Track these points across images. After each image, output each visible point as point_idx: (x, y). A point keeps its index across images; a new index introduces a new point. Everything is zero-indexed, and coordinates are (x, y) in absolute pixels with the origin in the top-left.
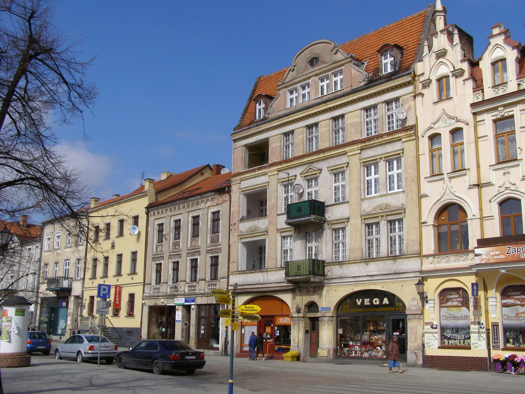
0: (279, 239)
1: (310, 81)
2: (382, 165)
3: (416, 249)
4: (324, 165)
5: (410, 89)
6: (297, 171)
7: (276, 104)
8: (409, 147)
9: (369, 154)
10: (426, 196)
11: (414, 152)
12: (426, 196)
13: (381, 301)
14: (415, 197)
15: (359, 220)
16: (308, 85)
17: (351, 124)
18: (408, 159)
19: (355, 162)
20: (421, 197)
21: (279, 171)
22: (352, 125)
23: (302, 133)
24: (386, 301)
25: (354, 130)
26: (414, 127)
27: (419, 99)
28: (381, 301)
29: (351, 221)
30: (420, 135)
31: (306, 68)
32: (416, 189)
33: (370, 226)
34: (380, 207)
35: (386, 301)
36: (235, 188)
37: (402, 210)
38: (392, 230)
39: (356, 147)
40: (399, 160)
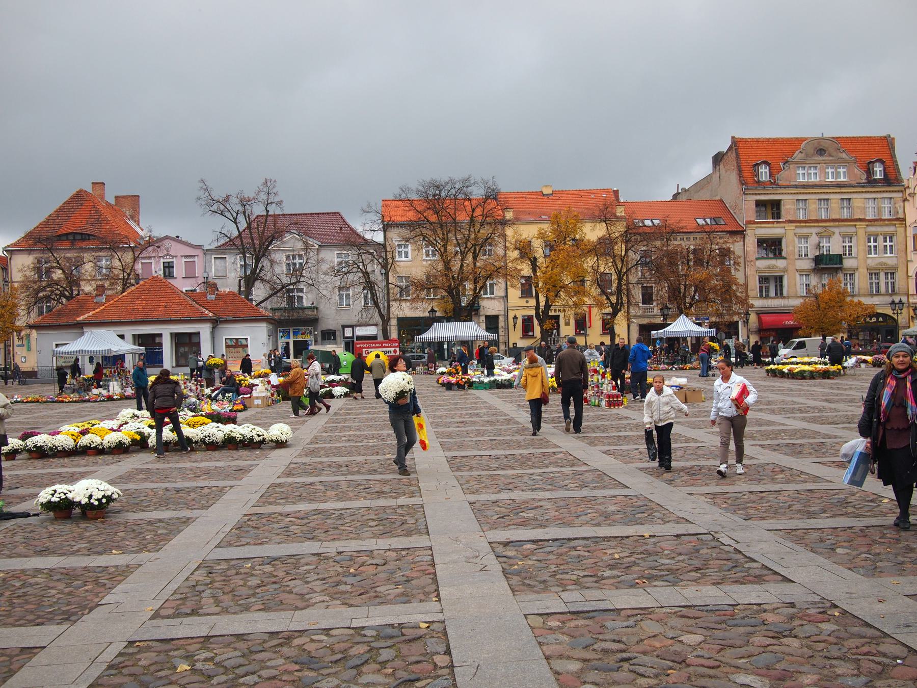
0: (798, 276)
1: (819, 166)
2: (881, 239)
3: (905, 290)
4: (837, 231)
5: (900, 195)
6: (814, 231)
7: (783, 174)
8: (900, 230)
9: (872, 229)
10: (911, 261)
11: (904, 234)
12: (911, 261)
13: (878, 319)
14: (905, 262)
15: (865, 271)
16: (816, 167)
17: (857, 207)
18: (897, 239)
19: (861, 233)
20: (907, 261)
21: (796, 227)
22: (858, 207)
23: (815, 203)
24: (881, 319)
25: (859, 211)
26: (904, 220)
27: (906, 203)
28: (878, 319)
29: (860, 270)
30: (907, 225)
31: (813, 155)
32: (905, 256)
33: (871, 274)
34: (880, 264)
35: (881, 319)
36: (749, 232)
37: (896, 268)
38: (887, 278)
39: (864, 223)
40: (891, 238)
